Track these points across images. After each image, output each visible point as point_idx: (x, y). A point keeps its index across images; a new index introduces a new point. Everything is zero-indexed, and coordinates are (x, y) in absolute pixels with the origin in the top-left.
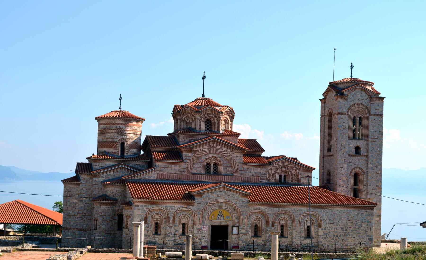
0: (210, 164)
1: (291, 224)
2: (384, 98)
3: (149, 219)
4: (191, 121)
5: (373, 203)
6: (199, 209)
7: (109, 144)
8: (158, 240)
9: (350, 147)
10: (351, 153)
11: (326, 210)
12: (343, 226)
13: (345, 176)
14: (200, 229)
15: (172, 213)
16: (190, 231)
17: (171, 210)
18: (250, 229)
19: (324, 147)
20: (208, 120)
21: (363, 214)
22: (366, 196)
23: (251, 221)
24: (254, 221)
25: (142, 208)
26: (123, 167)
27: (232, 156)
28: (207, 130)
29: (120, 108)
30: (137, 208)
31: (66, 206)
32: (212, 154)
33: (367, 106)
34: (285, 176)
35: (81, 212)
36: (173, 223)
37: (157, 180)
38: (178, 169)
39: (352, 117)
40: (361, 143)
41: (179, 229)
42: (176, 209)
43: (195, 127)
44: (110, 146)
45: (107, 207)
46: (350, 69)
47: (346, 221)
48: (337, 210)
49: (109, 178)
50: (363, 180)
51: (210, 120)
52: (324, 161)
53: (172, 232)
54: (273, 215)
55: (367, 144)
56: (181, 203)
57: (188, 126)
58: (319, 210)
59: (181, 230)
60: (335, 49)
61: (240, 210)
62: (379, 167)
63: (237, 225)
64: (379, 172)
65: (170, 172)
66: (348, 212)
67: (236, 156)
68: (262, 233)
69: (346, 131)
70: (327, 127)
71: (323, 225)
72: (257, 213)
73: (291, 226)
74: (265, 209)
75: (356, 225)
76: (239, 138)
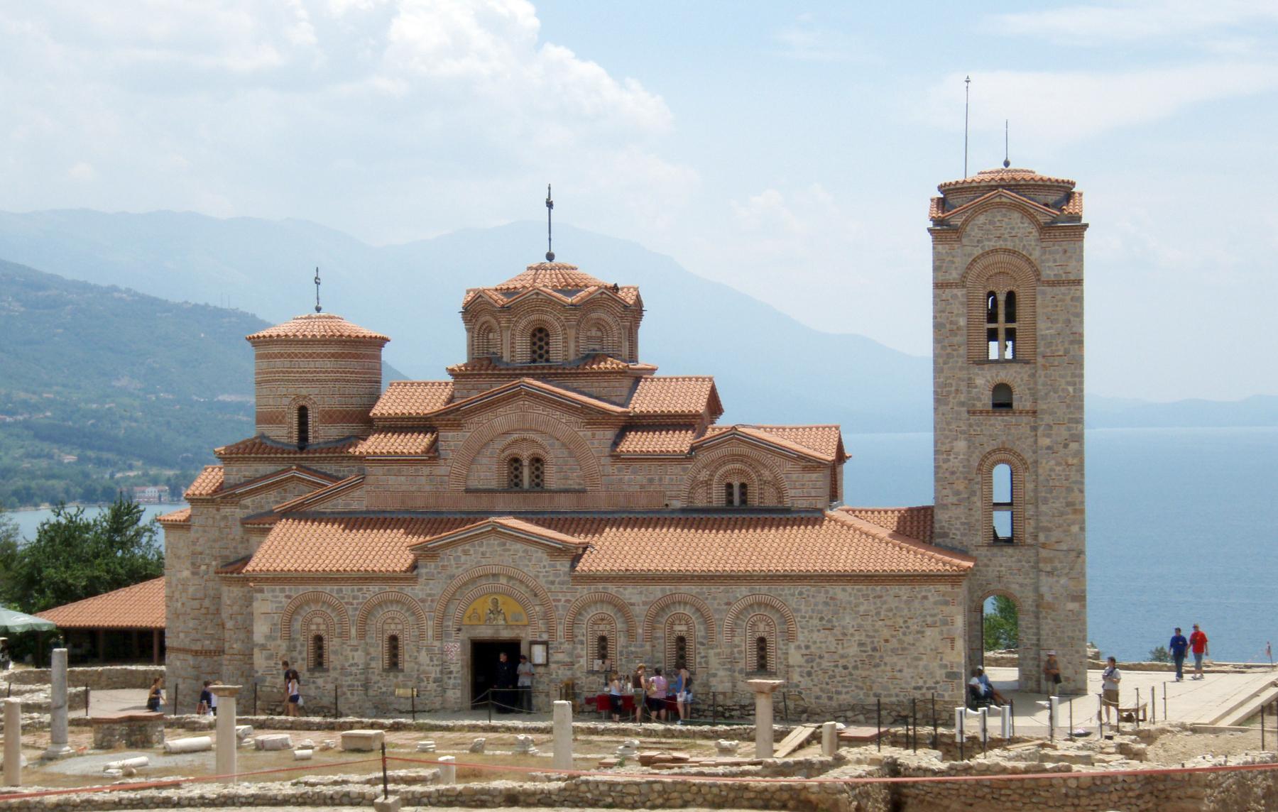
1: (703, 633)
6: (430, 595)
8: (323, 685)
9: (976, 387)
10: (979, 406)
12: (863, 638)
13: (962, 476)
14: (437, 652)
15: (356, 609)
16: (410, 656)
18: (582, 649)
20: (541, 330)
21: (925, 598)
22: (1036, 537)
23: (585, 626)
24: (596, 627)
25: (272, 596)
27: (581, 434)
28: (539, 360)
30: (259, 595)
33: (1031, 255)
34: (743, 486)
35: (196, 604)
36: (362, 635)
37: (368, 512)
38: (424, 478)
39: (982, 294)
41: (380, 651)
47: (873, 621)
48: (844, 590)
49: (262, 507)
54: (647, 607)
57: (491, 350)
58: (787, 591)
61: (549, 594)
62: (1074, 446)
63: (545, 637)
64: (1075, 461)
65: (404, 488)
66: (879, 593)
67: (590, 433)
68: (619, 663)
69: (960, 339)
72: (602, 602)
74: (621, 589)
75: (904, 634)
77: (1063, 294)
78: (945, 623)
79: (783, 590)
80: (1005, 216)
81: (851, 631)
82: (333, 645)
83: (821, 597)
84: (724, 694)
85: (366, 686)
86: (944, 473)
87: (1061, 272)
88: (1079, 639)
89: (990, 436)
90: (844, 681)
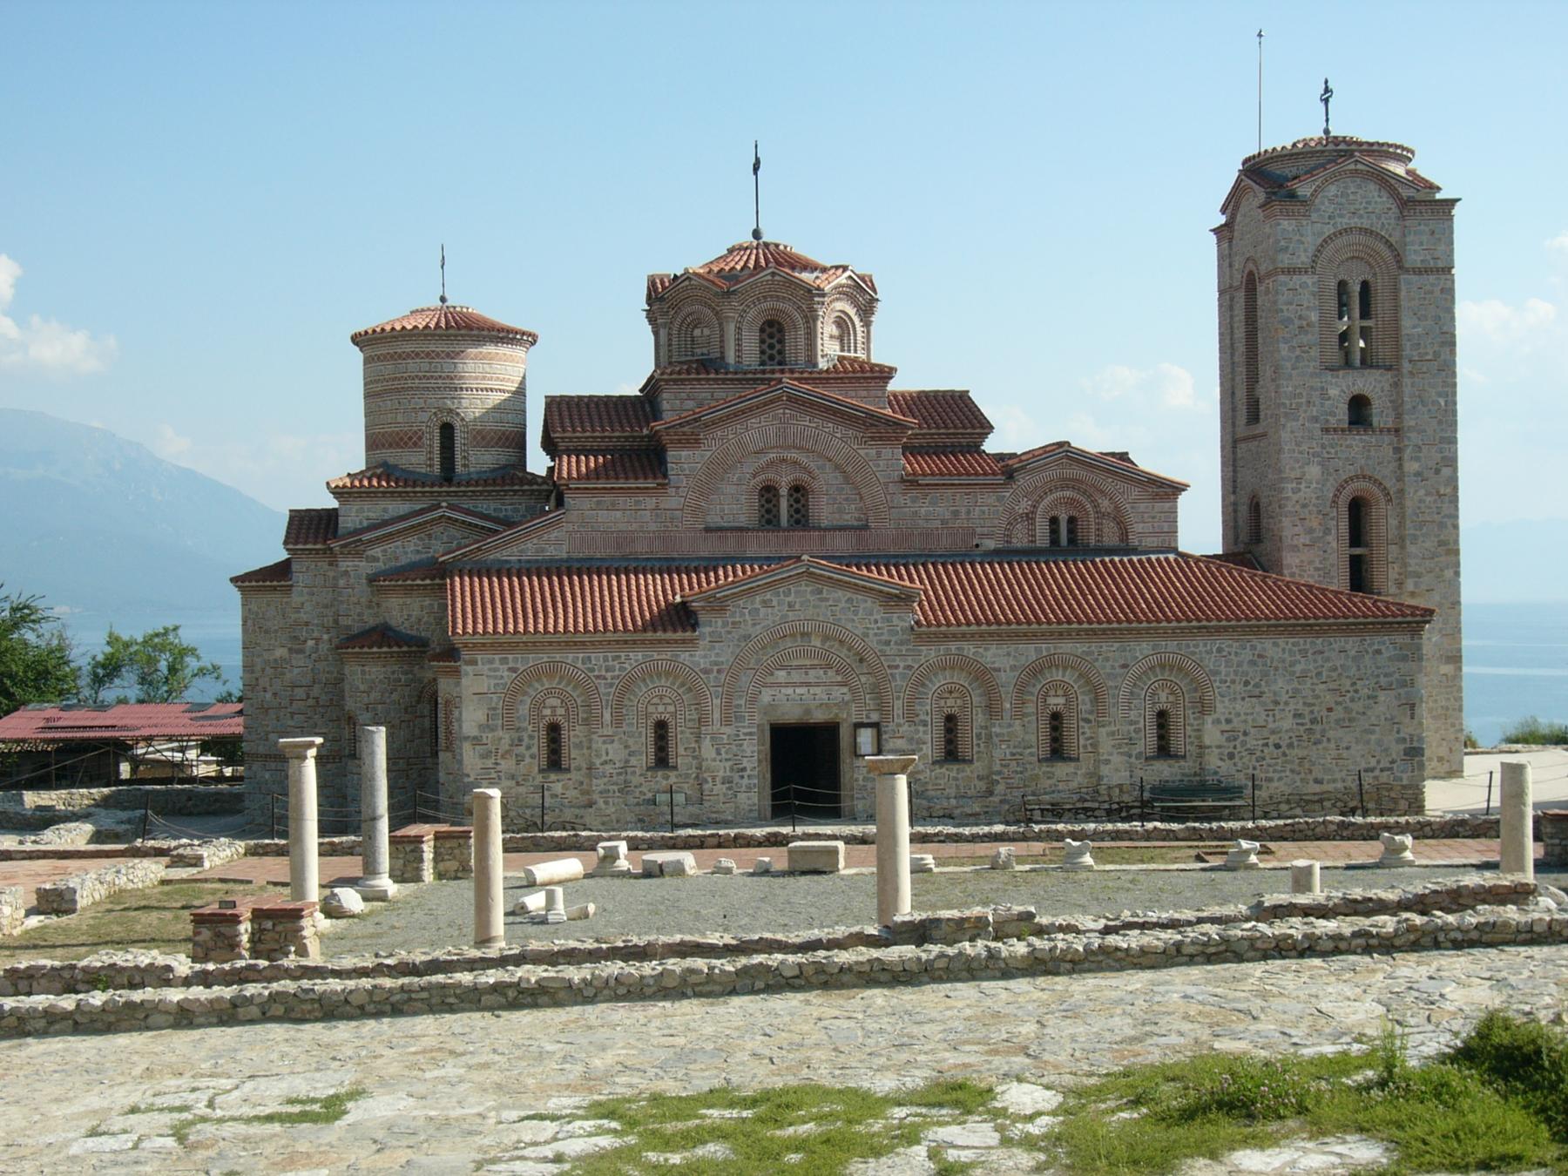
0: (775, 489)
1: (1088, 707)
2: (1452, 202)
3: (524, 710)
4: (706, 332)
5: (1417, 608)
6: (716, 664)
7: (398, 433)
9: (1329, 399)
11: (1227, 643)
12: (1300, 706)
15: (611, 685)
17: (607, 671)
19: (1234, 410)
20: (770, 323)
21: (1378, 652)
22: (1400, 584)
24: (942, 703)
25: (490, 670)
26: (450, 518)
29: (443, 299)
30: (469, 669)
31: (253, 672)
32: (781, 447)
34: (1072, 520)
36: (618, 721)
39: (1333, 284)
40: (1369, 383)
42: (626, 666)
43: (722, 353)
44: (401, 439)
45: (389, 669)
46: (1322, 105)
48: (1276, 645)
50: (1383, 521)
51: (779, 324)
52: (1235, 460)
53: (616, 759)
55: (1396, 385)
56: (643, 642)
57: (698, 351)
59: (652, 750)
60: (1260, 35)
62: (1446, 471)
63: (875, 717)
64: (1448, 490)
65: (622, 527)
67: (874, 451)
68: (975, 749)
69: (1312, 337)
70: (1240, 333)
71: (1218, 705)
73: (1091, 712)
74: (981, 650)
75: (1352, 700)
76: (894, 386)
77: (1432, 285)
78: (1403, 684)
79: (1196, 646)
80: (1359, 187)
81: (1284, 698)
82: (575, 736)
83: (1247, 655)
84: (1120, 786)
85: (625, 789)
86: (1294, 506)
87: (1428, 257)
88: (1454, 710)
89: (1347, 459)
90: (1277, 764)
